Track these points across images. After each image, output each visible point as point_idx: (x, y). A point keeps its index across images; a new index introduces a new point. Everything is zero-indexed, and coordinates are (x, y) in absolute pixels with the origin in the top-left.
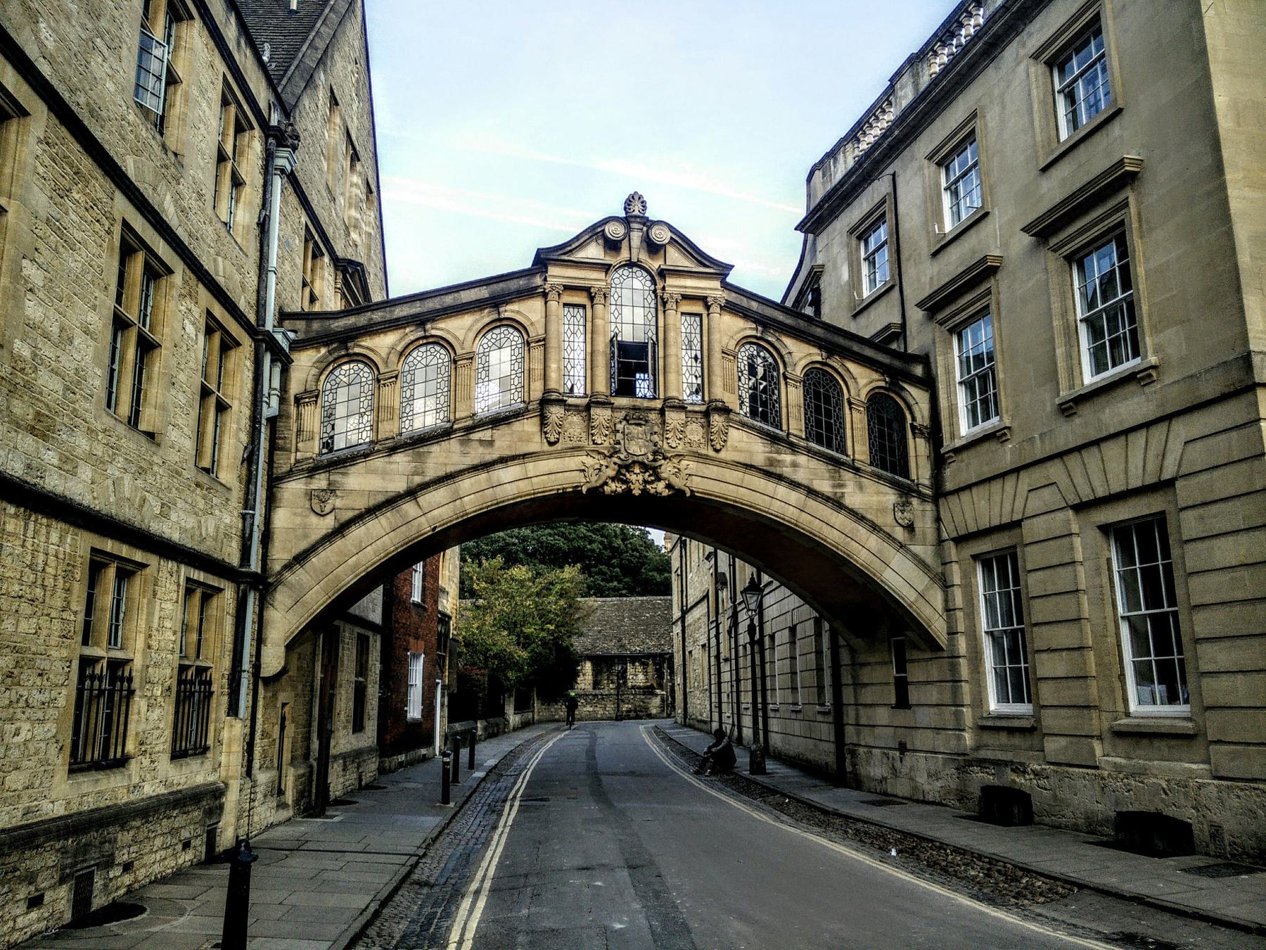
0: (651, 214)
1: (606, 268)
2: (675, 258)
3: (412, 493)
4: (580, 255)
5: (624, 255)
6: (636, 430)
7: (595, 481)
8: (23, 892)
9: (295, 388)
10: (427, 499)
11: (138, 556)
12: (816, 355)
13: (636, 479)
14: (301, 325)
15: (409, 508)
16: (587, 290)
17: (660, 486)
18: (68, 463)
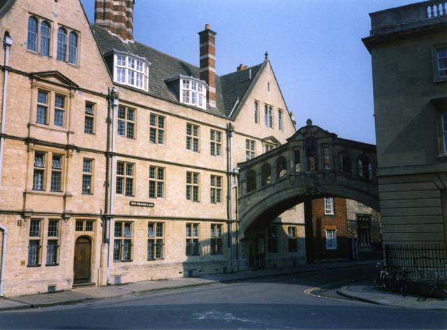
0: (313, 124)
1: (303, 140)
2: (319, 134)
3: (264, 200)
4: (296, 139)
5: (308, 135)
6: (312, 180)
7: (303, 193)
8: (178, 272)
9: (241, 179)
10: (267, 201)
11: (197, 222)
12: (362, 153)
13: (313, 192)
14: (241, 165)
15: (264, 203)
16: (298, 147)
17: (318, 193)
18: (180, 212)
